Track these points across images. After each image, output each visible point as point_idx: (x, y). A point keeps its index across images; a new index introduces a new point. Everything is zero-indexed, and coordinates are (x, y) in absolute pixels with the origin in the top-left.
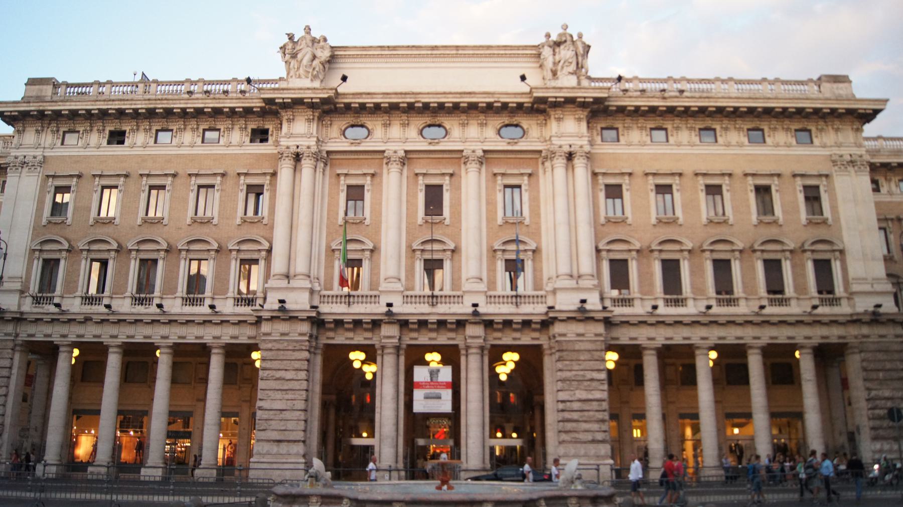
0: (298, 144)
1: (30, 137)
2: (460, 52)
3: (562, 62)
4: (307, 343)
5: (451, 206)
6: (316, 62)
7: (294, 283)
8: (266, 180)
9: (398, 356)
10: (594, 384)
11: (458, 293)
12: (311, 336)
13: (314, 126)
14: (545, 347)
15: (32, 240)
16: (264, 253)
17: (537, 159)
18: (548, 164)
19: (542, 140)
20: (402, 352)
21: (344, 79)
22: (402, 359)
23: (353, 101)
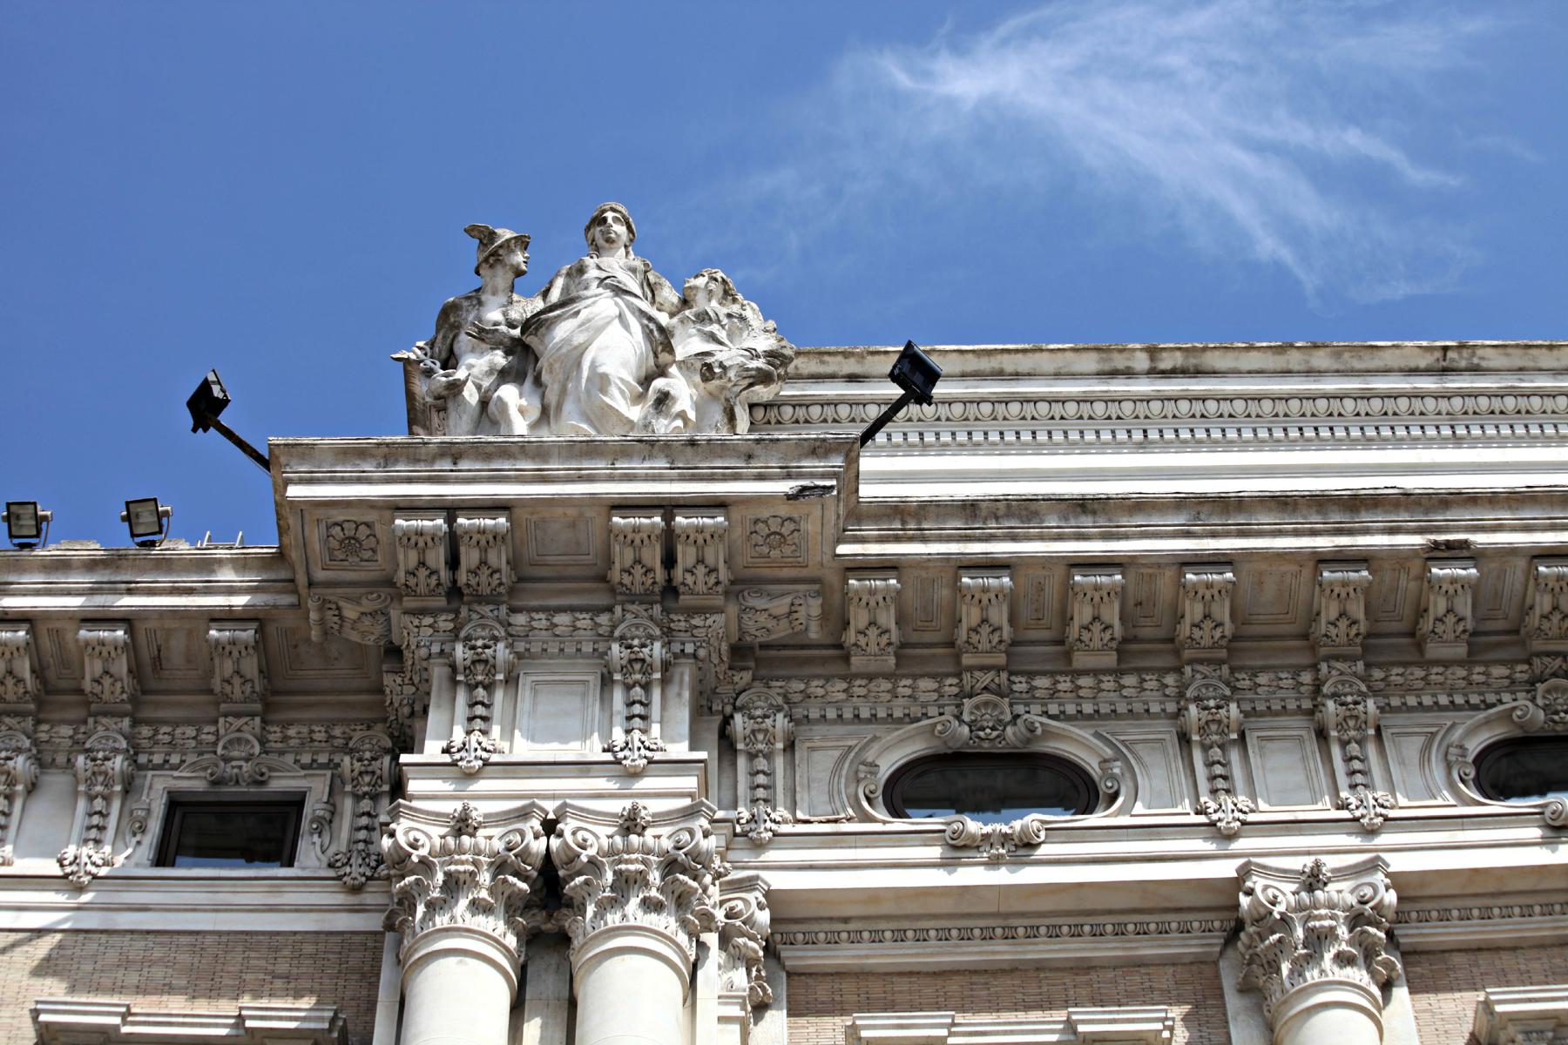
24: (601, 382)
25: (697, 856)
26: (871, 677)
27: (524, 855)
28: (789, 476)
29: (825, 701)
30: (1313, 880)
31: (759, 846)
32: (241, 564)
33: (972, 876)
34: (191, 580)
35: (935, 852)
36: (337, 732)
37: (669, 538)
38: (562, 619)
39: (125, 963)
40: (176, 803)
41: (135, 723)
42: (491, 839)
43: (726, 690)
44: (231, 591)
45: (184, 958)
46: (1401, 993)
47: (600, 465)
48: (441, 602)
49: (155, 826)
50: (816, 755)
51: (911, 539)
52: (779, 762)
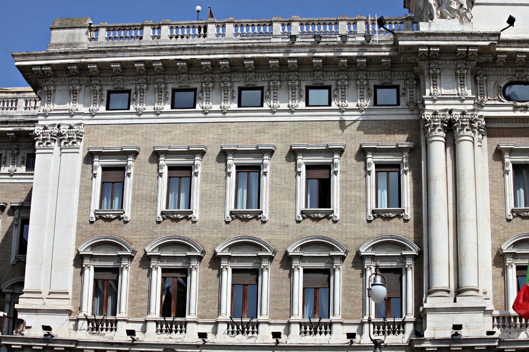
0: (450, 107)
1: (19, 94)
7: (463, 302)
8: (404, 159)
13: (468, 81)
15: (78, 243)
16: (409, 262)
21: (511, 21)
23: (520, 50)
28: (489, 41)
29: (492, 71)
32: (387, 46)
33: (518, 114)
34: (378, 49)
35: (511, 108)
36: (405, 73)
37: (467, 52)
38: (448, 62)
39: (373, 128)
42: (441, 116)
43: (476, 70)
44: (385, 51)
45: (383, 126)
47: (455, 38)
50: (491, 82)
51: (509, 47)
52: (485, 85)
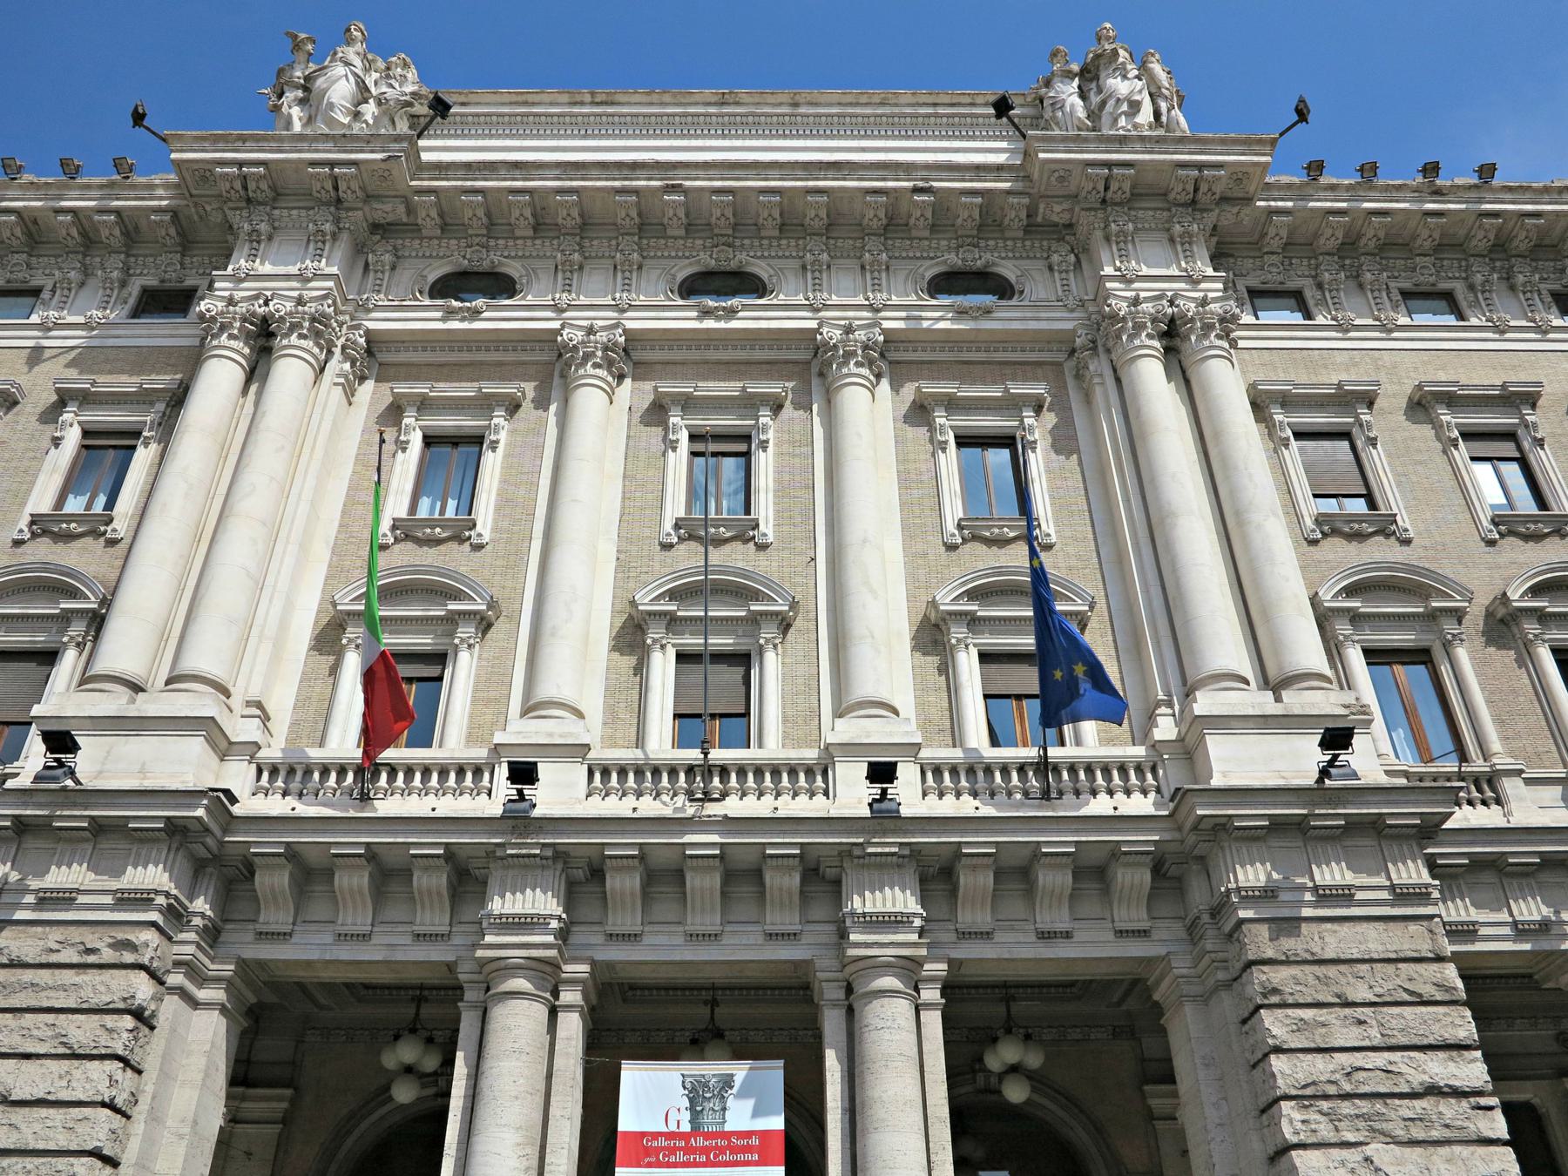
2: (802, 110)
3: (1111, 102)
4: (150, 936)
5: (781, 491)
6: (370, 110)
9: (553, 1012)
10: (1450, 1109)
11: (810, 754)
12: (177, 915)
14: (1181, 966)
17: (1059, 364)
18: (1098, 366)
19: (1071, 302)
20: (570, 996)
22: (572, 1027)
24: (331, 106)
25: (324, 315)
26: (431, 238)
27: (254, 314)
30: (590, 331)
31: (369, 311)
32: (166, 186)
34: (145, 193)
35: (439, 314)
38: (294, 212)
39: (107, 361)
40: (146, 291)
41: (128, 255)
44: (161, 198)
46: (628, 382)
48: (244, 204)
49: (132, 301)
